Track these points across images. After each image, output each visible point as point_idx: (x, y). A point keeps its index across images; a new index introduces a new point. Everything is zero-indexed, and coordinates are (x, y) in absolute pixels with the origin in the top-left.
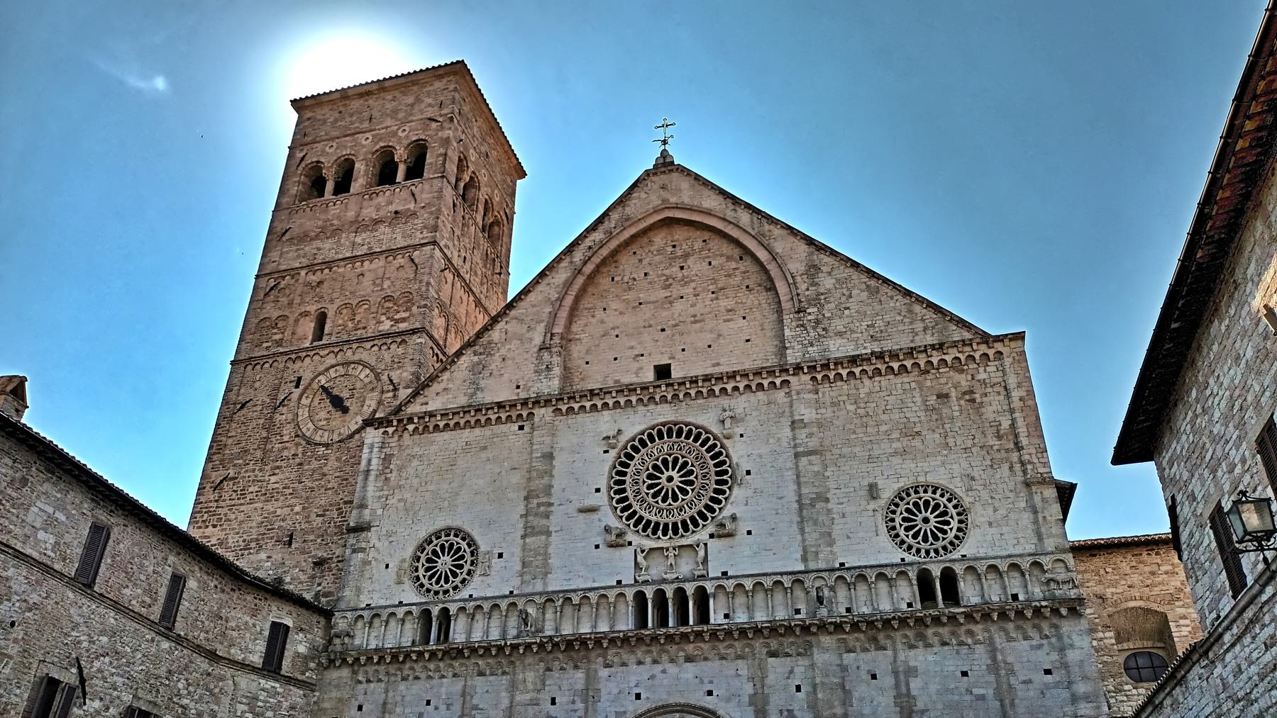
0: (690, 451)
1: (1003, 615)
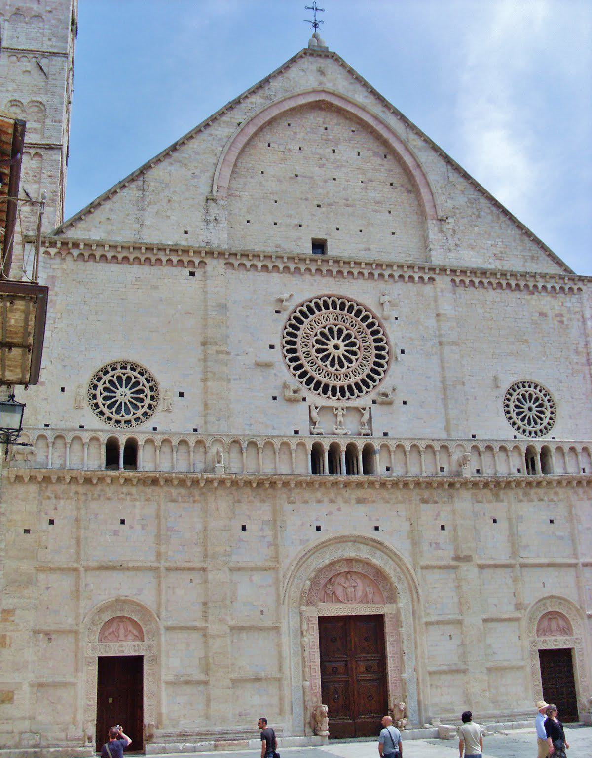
0: (350, 323)
1: (579, 483)
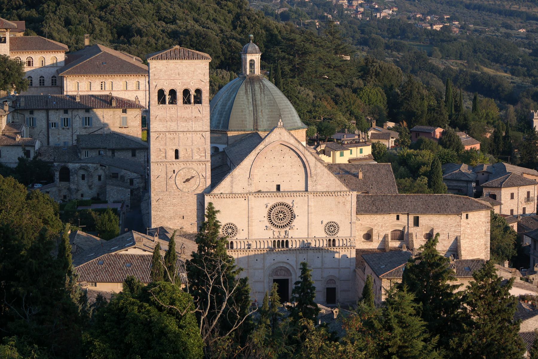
0: (285, 209)
